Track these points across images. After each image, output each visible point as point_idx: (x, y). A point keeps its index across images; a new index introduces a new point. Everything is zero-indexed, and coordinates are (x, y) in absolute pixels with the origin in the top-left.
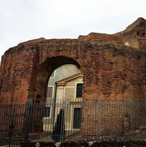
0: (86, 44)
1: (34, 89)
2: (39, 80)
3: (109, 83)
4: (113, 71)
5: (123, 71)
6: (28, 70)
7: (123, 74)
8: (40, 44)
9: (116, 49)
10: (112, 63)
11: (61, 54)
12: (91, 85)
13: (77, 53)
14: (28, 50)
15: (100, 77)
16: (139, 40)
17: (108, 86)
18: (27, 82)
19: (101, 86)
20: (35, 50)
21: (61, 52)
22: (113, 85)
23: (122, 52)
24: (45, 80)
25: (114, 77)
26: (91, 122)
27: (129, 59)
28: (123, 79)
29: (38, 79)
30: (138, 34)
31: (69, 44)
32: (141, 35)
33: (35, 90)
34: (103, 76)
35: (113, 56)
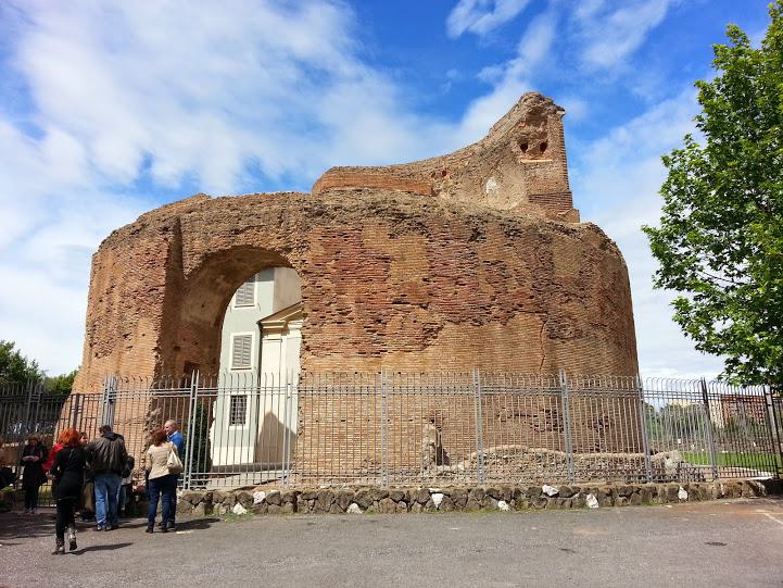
0: (309, 206)
3: (380, 321)
4: (390, 283)
5: (425, 280)
6: (154, 292)
7: (423, 290)
8: (187, 216)
10: (386, 259)
11: (242, 240)
13: (285, 236)
14: (153, 235)
16: (526, 167)
17: (375, 331)
18: (152, 327)
19: (353, 330)
20: (170, 236)
21: (241, 236)
23: (420, 224)
24: (209, 317)
28: (424, 308)
30: (524, 147)
33: (177, 349)
34: (358, 301)
35: (392, 236)
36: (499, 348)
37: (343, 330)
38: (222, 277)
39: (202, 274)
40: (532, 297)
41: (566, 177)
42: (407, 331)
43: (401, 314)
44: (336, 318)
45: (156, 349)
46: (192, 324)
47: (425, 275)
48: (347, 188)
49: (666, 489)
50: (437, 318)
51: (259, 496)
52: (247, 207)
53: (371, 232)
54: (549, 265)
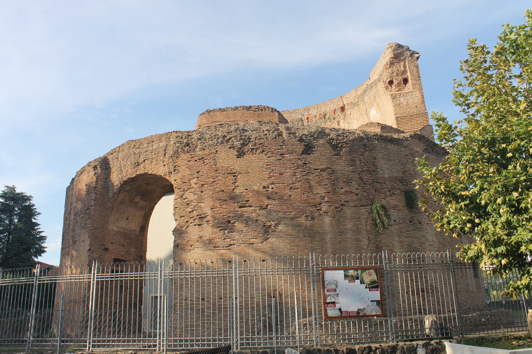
1: (103, 247)
2: (116, 229)
20: (99, 170)
21: (142, 166)
29: (113, 227)
31: (155, 147)
32: (399, 85)
41: (423, 102)
44: (197, 222)
45: (89, 250)
46: (119, 232)
47: (265, 184)
49: (405, 347)
52: (146, 145)
54: (372, 168)
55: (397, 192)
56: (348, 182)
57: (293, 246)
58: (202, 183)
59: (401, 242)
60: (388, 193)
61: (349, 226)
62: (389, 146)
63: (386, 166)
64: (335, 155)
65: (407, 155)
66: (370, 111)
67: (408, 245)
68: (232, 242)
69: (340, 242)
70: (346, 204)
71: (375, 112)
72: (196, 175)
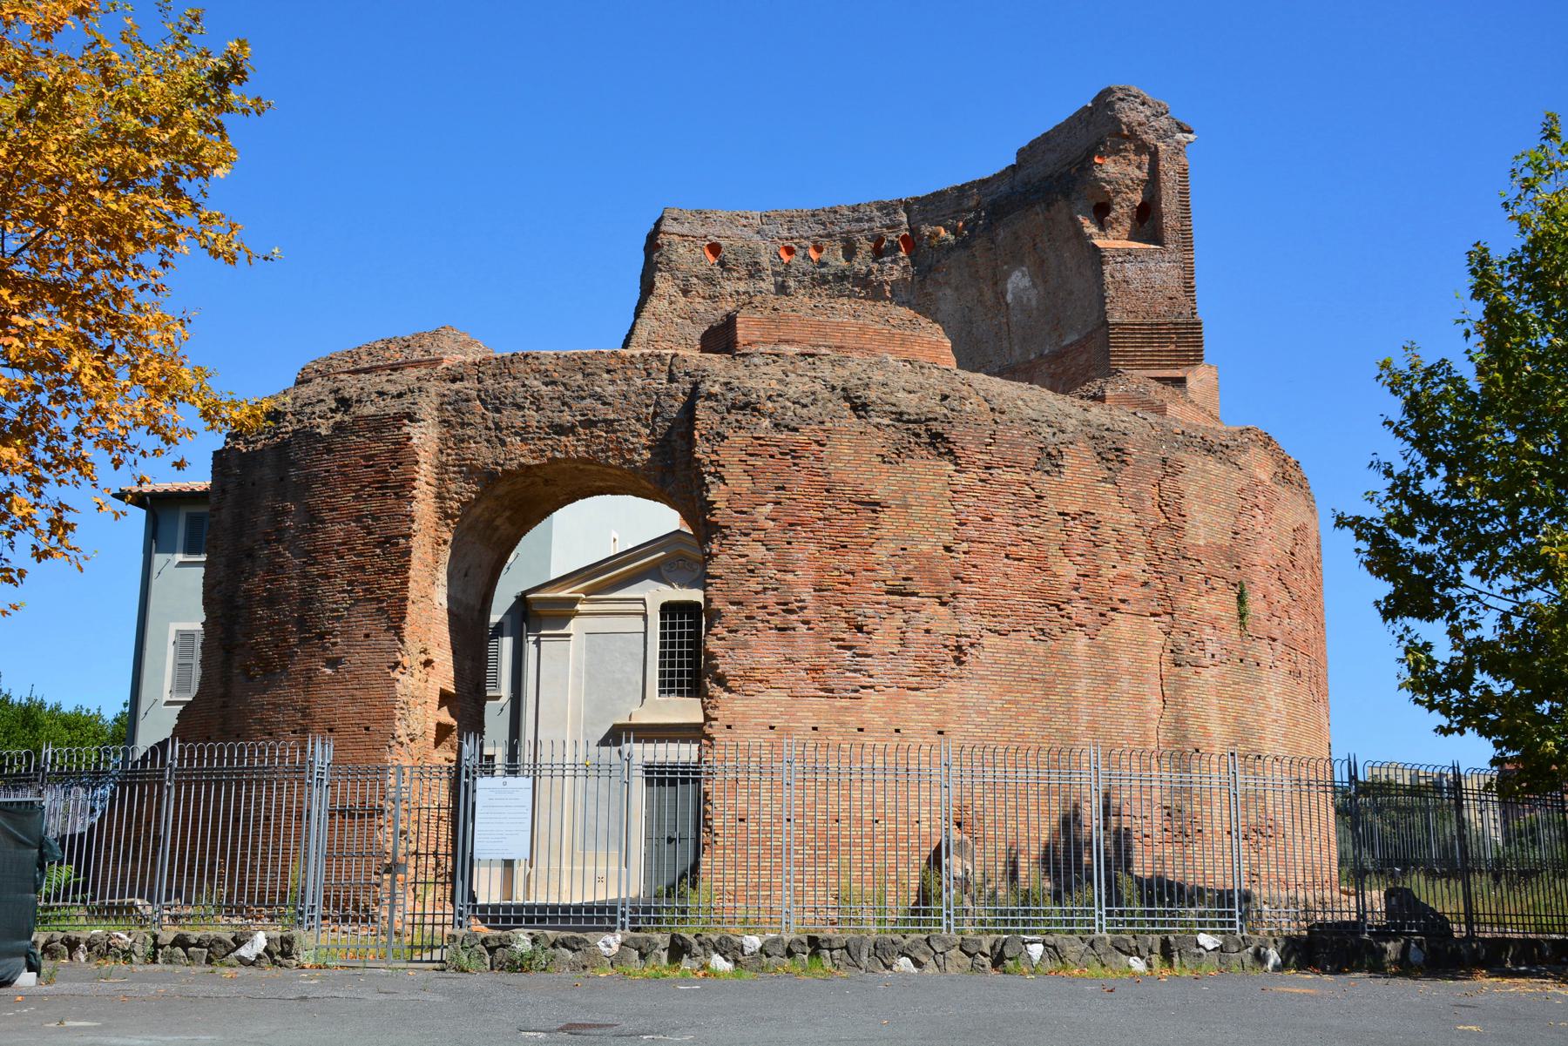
1: (423, 657)
3: (860, 629)
4: (881, 553)
5: (948, 549)
7: (944, 571)
9: (901, 414)
10: (875, 506)
12: (753, 640)
15: (807, 595)
17: (850, 648)
22: (883, 638)
25: (888, 593)
26: (753, 850)
27: (984, 476)
36: (1082, 686)
37: (791, 644)
38: (507, 514)
39: (478, 511)
40: (1145, 584)
41: (1189, 288)
42: (912, 650)
43: (899, 614)
47: (947, 538)
48: (784, 348)
50: (969, 625)
51: (753, 942)
53: (845, 451)
55: (1219, 584)
56: (1124, 555)
57: (1009, 702)
58: (791, 519)
59: (1223, 709)
60: (1203, 587)
61: (1125, 661)
62: (1210, 466)
63: (1201, 517)
64: (1105, 480)
65: (1242, 490)
66: (1008, 275)
67: (1235, 718)
68: (866, 681)
69: (1106, 700)
70: (1122, 606)
71: (1026, 282)
72: (771, 496)
